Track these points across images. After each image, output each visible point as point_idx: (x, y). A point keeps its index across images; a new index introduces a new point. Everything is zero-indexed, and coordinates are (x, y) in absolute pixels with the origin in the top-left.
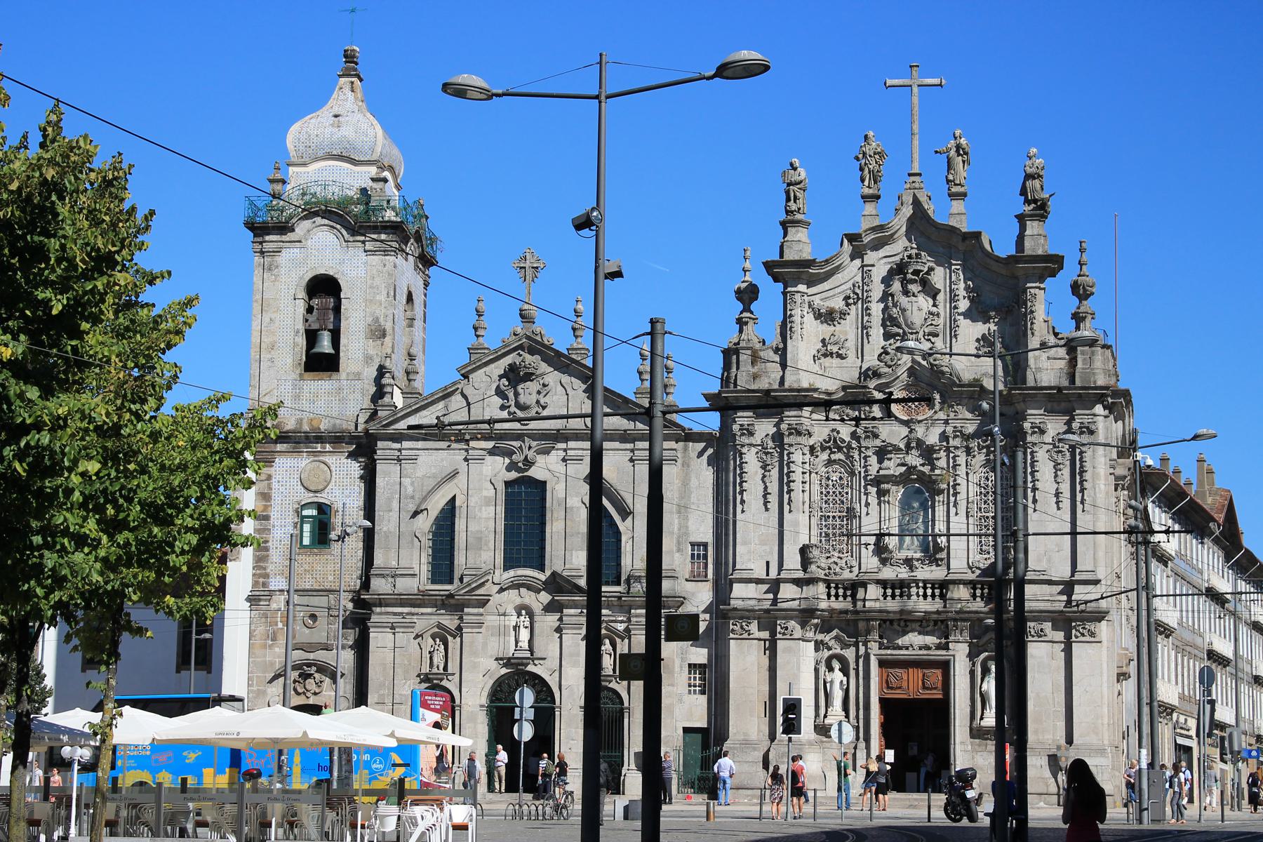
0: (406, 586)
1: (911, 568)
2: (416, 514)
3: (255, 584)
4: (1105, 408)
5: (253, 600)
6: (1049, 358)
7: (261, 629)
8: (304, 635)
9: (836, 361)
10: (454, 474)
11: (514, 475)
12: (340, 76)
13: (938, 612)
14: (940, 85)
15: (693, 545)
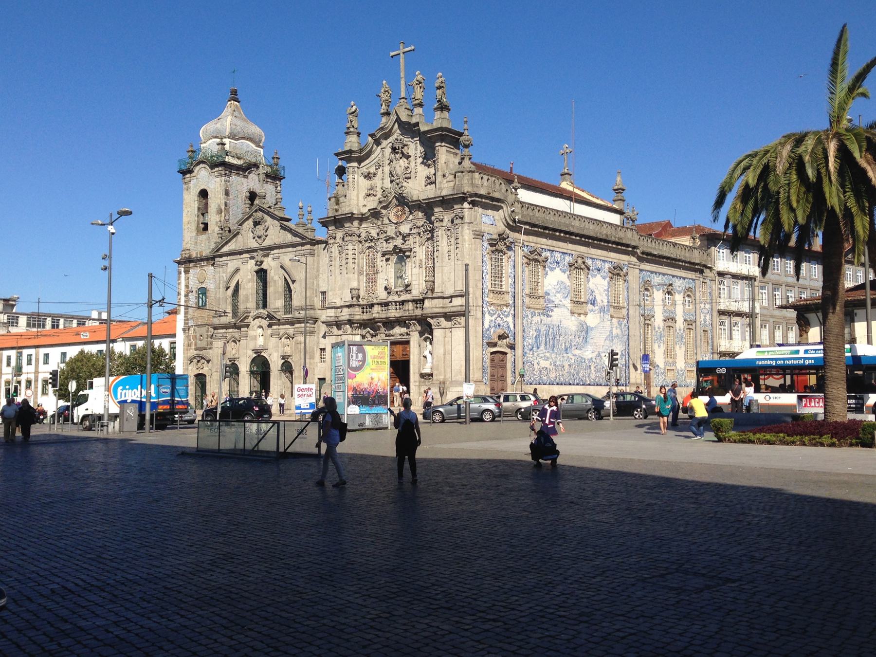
0: (224, 320)
1: (399, 296)
2: (227, 290)
3: (185, 323)
4: (469, 203)
5: (184, 330)
6: (447, 182)
7: (186, 342)
8: (200, 344)
9: (372, 198)
10: (237, 270)
11: (257, 268)
12: (228, 101)
13: (400, 317)
14: (414, 50)
15: (322, 293)
